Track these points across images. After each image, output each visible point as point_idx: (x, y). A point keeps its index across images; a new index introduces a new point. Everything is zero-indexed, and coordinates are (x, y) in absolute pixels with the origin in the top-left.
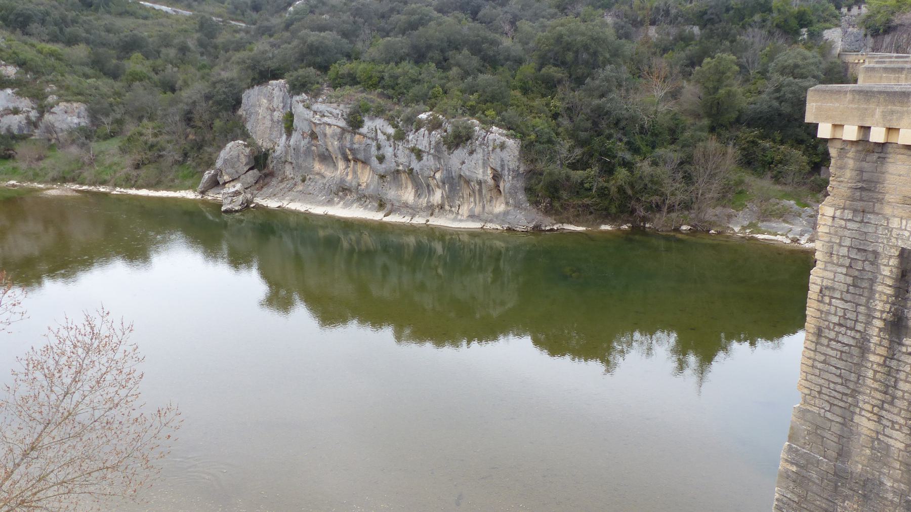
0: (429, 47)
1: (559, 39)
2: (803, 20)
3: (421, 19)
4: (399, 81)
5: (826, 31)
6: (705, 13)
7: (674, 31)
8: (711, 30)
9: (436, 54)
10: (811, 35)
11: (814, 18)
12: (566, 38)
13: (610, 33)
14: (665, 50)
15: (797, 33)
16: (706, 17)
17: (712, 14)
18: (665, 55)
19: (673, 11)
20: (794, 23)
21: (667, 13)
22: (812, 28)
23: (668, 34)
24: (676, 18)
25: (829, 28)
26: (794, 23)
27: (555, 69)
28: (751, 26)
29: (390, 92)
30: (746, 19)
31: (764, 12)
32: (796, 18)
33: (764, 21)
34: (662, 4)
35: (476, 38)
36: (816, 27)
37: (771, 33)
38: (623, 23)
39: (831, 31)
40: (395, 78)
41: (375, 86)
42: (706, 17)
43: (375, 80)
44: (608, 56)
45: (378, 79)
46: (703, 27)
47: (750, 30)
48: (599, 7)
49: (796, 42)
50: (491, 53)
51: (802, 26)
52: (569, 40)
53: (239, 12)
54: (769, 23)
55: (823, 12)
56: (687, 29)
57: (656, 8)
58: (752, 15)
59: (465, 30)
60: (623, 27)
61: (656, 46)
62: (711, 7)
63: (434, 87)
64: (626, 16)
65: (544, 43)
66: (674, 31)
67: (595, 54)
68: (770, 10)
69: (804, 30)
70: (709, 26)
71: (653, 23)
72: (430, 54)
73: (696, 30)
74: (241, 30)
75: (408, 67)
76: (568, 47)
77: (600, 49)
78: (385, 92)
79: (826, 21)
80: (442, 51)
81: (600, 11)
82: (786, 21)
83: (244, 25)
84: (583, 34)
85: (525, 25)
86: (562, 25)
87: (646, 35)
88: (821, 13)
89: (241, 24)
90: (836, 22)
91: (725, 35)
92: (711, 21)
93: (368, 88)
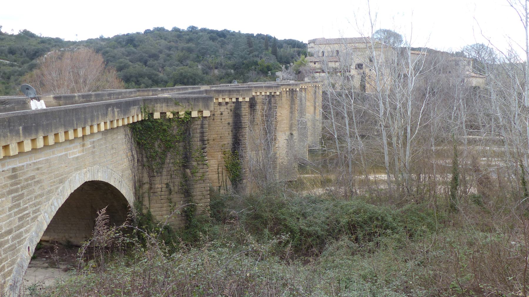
0: (131, 76)
1: (181, 74)
2: (269, 68)
3: (125, 65)
6: (235, 65)
7: (224, 71)
8: (237, 71)
9: (134, 79)
10: (272, 73)
11: (273, 68)
12: (184, 74)
13: (200, 72)
14: (221, 79)
15: (267, 73)
16: (235, 67)
18: (221, 80)
19: (224, 64)
20: (266, 69)
21: (221, 65)
23: (222, 73)
24: (225, 66)
25: (278, 72)
26: (266, 69)
28: (252, 70)
30: (250, 68)
31: (256, 65)
32: (267, 68)
33: (256, 68)
34: (219, 62)
36: (273, 71)
37: (258, 73)
38: (205, 68)
39: (278, 72)
42: (235, 67)
44: (199, 80)
46: (235, 70)
48: (196, 62)
49: (267, 76)
50: (156, 79)
51: (269, 71)
52: (185, 74)
53: (3, 55)
54: (257, 69)
55: (276, 65)
56: (229, 70)
57: (217, 63)
59: (144, 70)
60: (205, 70)
61: (218, 77)
62: (237, 63)
65: (176, 76)
66: (224, 71)
67: (195, 79)
68: (258, 65)
69: (269, 72)
70: (236, 70)
71: (216, 68)
73: (232, 71)
74: (6, 64)
76: (185, 77)
77: (196, 78)
79: (277, 69)
80: (136, 78)
81: (196, 63)
82: (263, 69)
83: (8, 62)
84: (190, 73)
85: (168, 69)
86: (182, 69)
87: (214, 73)
89: (6, 61)
90: (280, 69)
91: (242, 73)
92: (237, 68)
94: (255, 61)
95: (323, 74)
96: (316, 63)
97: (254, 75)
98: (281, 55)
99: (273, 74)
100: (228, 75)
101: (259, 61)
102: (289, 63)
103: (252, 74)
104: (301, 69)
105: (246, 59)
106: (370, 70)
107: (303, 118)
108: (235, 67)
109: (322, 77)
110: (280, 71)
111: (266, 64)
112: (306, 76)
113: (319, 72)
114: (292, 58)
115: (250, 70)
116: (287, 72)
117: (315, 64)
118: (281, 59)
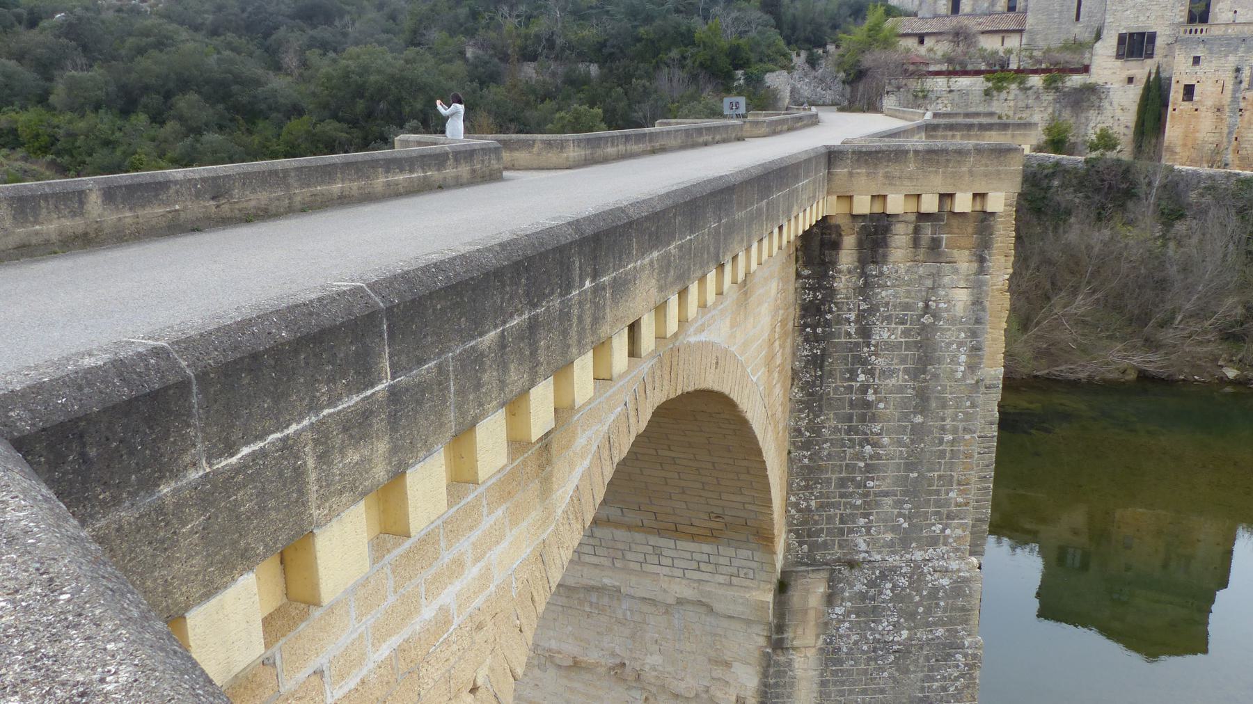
0: (146, 89)
2: (737, 58)
4: (78, 144)
5: (768, 75)
6: (603, 45)
7: (561, 70)
8: (611, 70)
9: (155, 100)
10: (748, 79)
12: (354, 77)
15: (730, 77)
16: (605, 51)
17: (613, 46)
19: (559, 41)
20: (724, 62)
21: (551, 44)
22: (749, 70)
24: (563, 49)
25: (772, 71)
26: (724, 62)
27: (337, 125)
29: (66, 159)
32: (728, 55)
35: (223, 76)
36: (754, 70)
37: (694, 78)
39: (774, 74)
40: (72, 135)
41: (45, 150)
43: (44, 139)
45: (46, 138)
47: (666, 70)
50: (244, 99)
51: (737, 67)
55: (769, 46)
56: (581, 67)
58: (669, 49)
59: (212, 60)
60: (486, 63)
63: (135, 153)
64: (494, 47)
66: (561, 70)
68: (693, 43)
69: (739, 73)
70: (607, 65)
72: (144, 100)
73: (594, 69)
75: (104, 122)
78: (59, 160)
79: (772, 60)
82: (713, 58)
88: (763, 48)
90: (786, 62)
93: (35, 153)
94: (683, 29)
95: (963, 82)
96: (926, 40)
97: (675, 84)
98: (794, 16)
99: (755, 81)
100: (576, 83)
101: (701, 29)
102: (823, 45)
103: (669, 82)
104: (867, 60)
105: (649, 19)
106: (1197, 60)
107: (934, 541)
108: (601, 52)
109: (964, 94)
110: (783, 68)
111: (727, 39)
112: (887, 88)
113: (950, 73)
114: (835, 27)
115: (662, 66)
116: (815, 77)
117: (921, 42)
118: (794, 28)
